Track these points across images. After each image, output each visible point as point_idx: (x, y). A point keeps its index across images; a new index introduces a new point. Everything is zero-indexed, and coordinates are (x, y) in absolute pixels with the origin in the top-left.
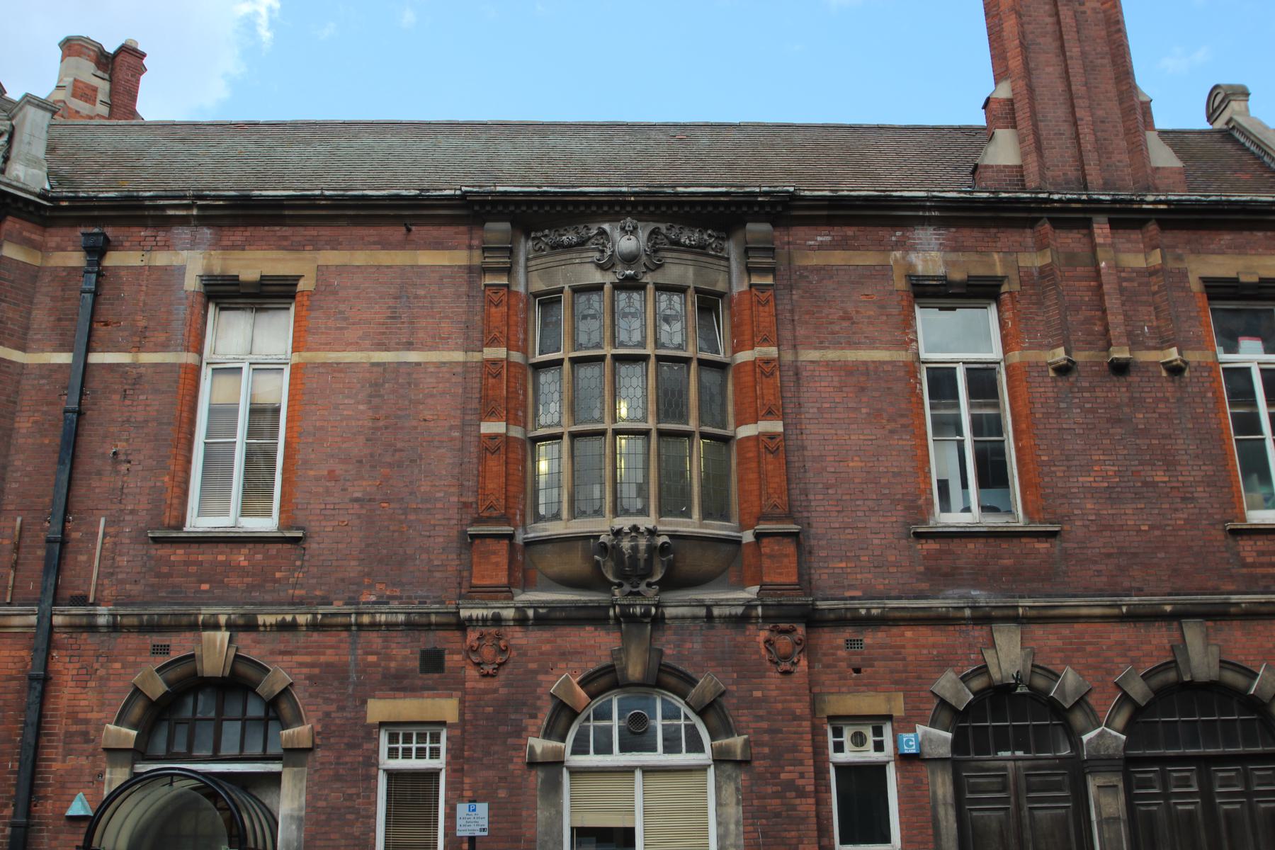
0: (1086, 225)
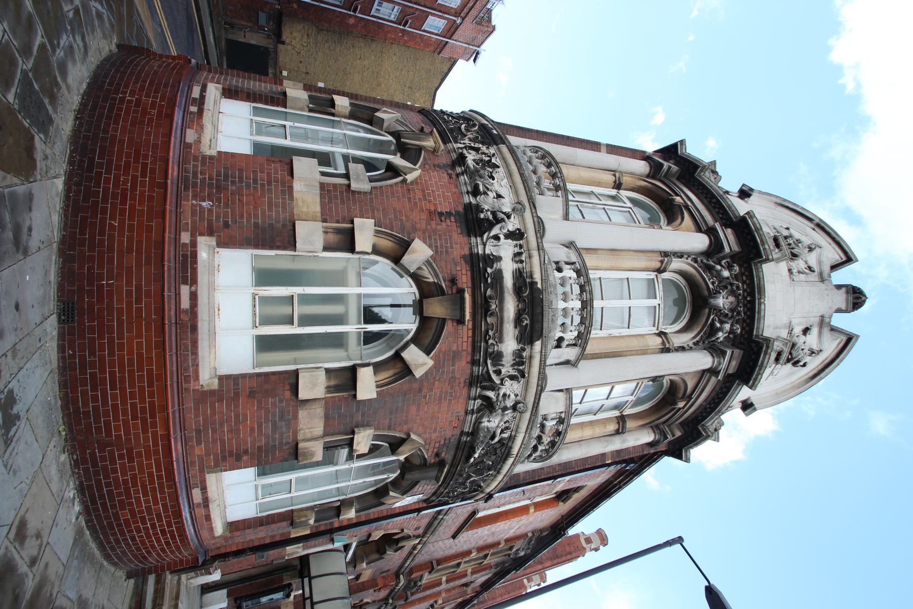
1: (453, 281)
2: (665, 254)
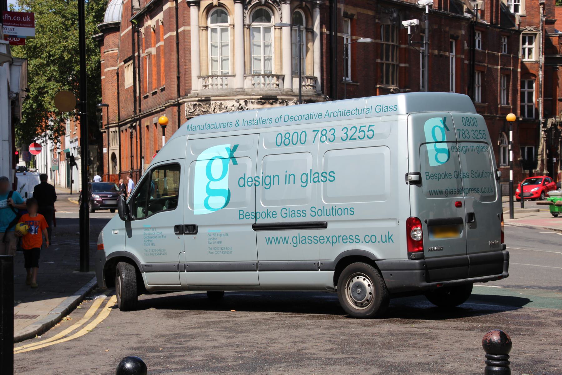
2: (244, 25)
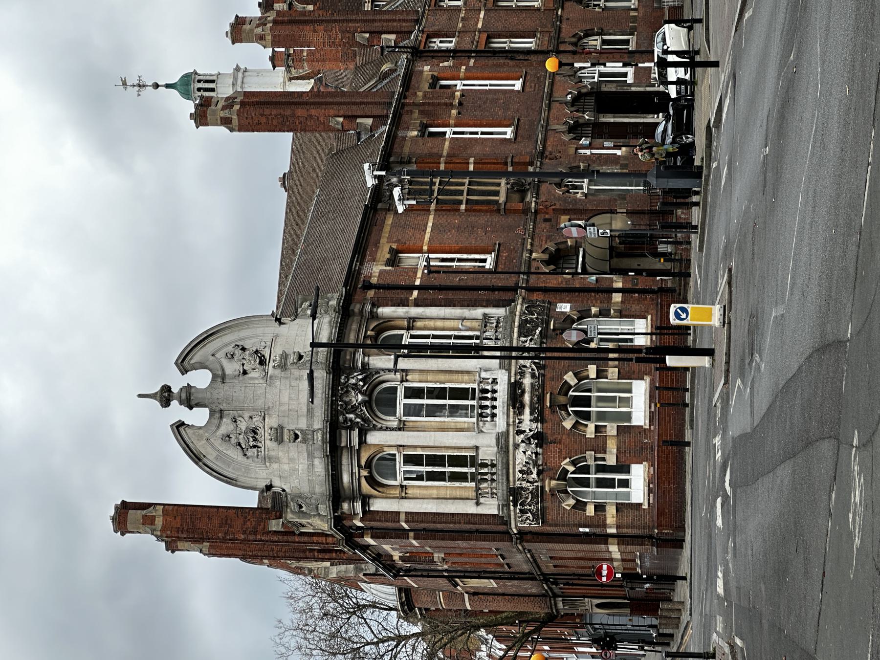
0: (404, 105)
1: (553, 412)
